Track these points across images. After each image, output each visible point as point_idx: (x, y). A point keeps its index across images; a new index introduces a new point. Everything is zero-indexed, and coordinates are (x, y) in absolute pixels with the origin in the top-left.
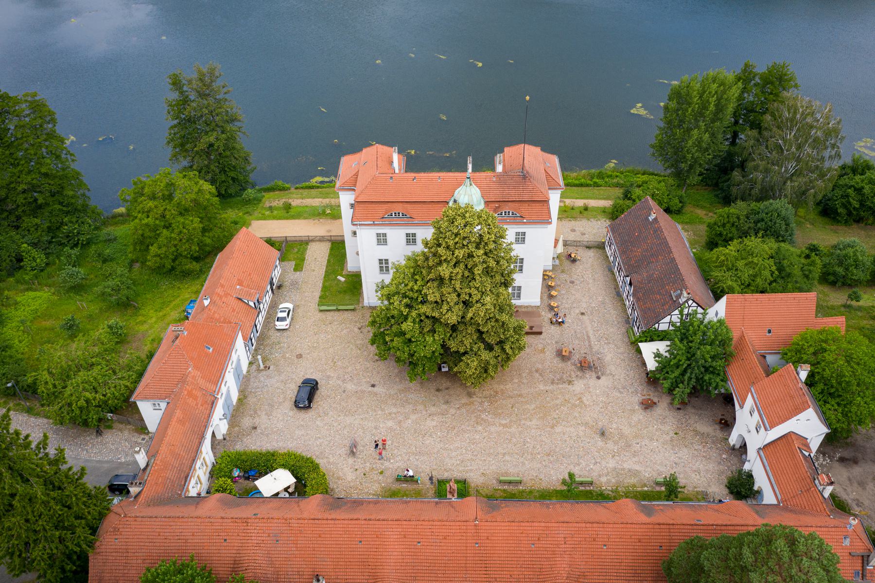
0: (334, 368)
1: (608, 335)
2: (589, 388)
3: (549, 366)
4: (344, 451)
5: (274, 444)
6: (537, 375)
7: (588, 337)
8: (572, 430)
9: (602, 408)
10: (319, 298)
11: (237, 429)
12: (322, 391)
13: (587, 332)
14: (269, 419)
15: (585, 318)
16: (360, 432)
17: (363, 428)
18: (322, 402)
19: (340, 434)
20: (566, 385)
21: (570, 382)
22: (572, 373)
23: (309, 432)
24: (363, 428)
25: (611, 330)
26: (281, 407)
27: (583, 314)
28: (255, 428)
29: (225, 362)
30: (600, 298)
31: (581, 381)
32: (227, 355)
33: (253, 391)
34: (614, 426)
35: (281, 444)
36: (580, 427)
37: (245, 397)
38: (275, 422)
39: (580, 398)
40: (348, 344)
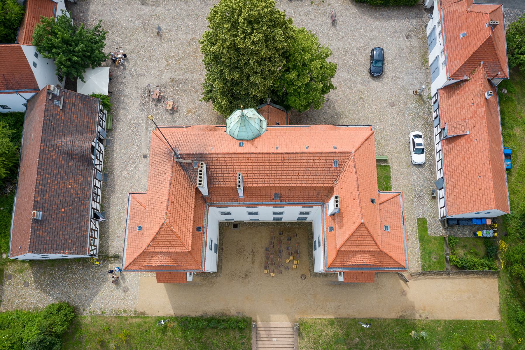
0: (361, 93)
1: (129, 128)
2: (159, 75)
3: (186, 96)
4: (340, 19)
5: (390, 25)
6: (197, 87)
7: (146, 129)
8: (179, 36)
9: (154, 55)
10: (390, 177)
11: (420, 36)
12: (365, 70)
13: (147, 134)
14: (399, 45)
15: (144, 152)
16: (331, 34)
17: (329, 37)
18: (363, 60)
19: (345, 32)
20: (176, 78)
21: (172, 81)
22: (168, 90)
23: (367, 34)
24: (329, 37)
25: (124, 134)
26: (393, 55)
27: (145, 157)
28: (407, 38)
29: (446, 37)
30: (124, 173)
31: (164, 82)
32: (446, 43)
33: (419, 70)
34: (149, 39)
35: (385, 24)
36: (174, 39)
37: (423, 64)
38: (394, 42)
39: (168, 65)
40: (353, 118)
